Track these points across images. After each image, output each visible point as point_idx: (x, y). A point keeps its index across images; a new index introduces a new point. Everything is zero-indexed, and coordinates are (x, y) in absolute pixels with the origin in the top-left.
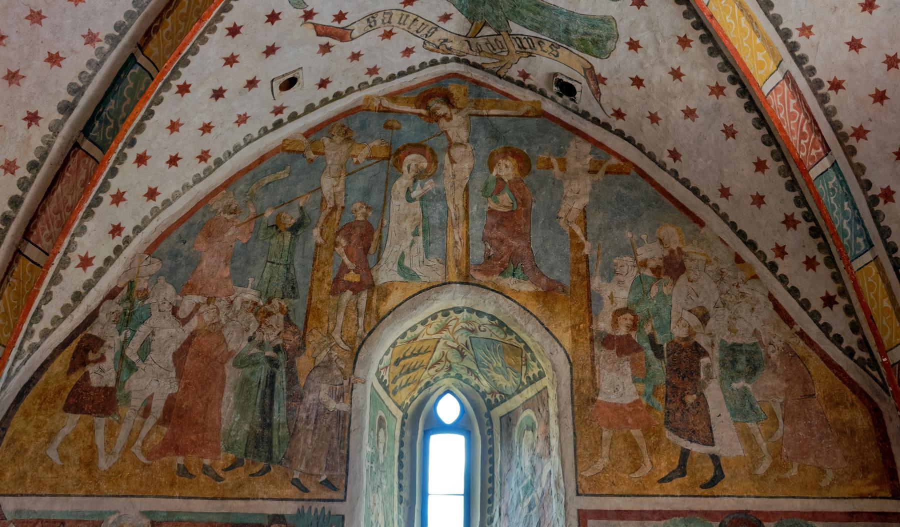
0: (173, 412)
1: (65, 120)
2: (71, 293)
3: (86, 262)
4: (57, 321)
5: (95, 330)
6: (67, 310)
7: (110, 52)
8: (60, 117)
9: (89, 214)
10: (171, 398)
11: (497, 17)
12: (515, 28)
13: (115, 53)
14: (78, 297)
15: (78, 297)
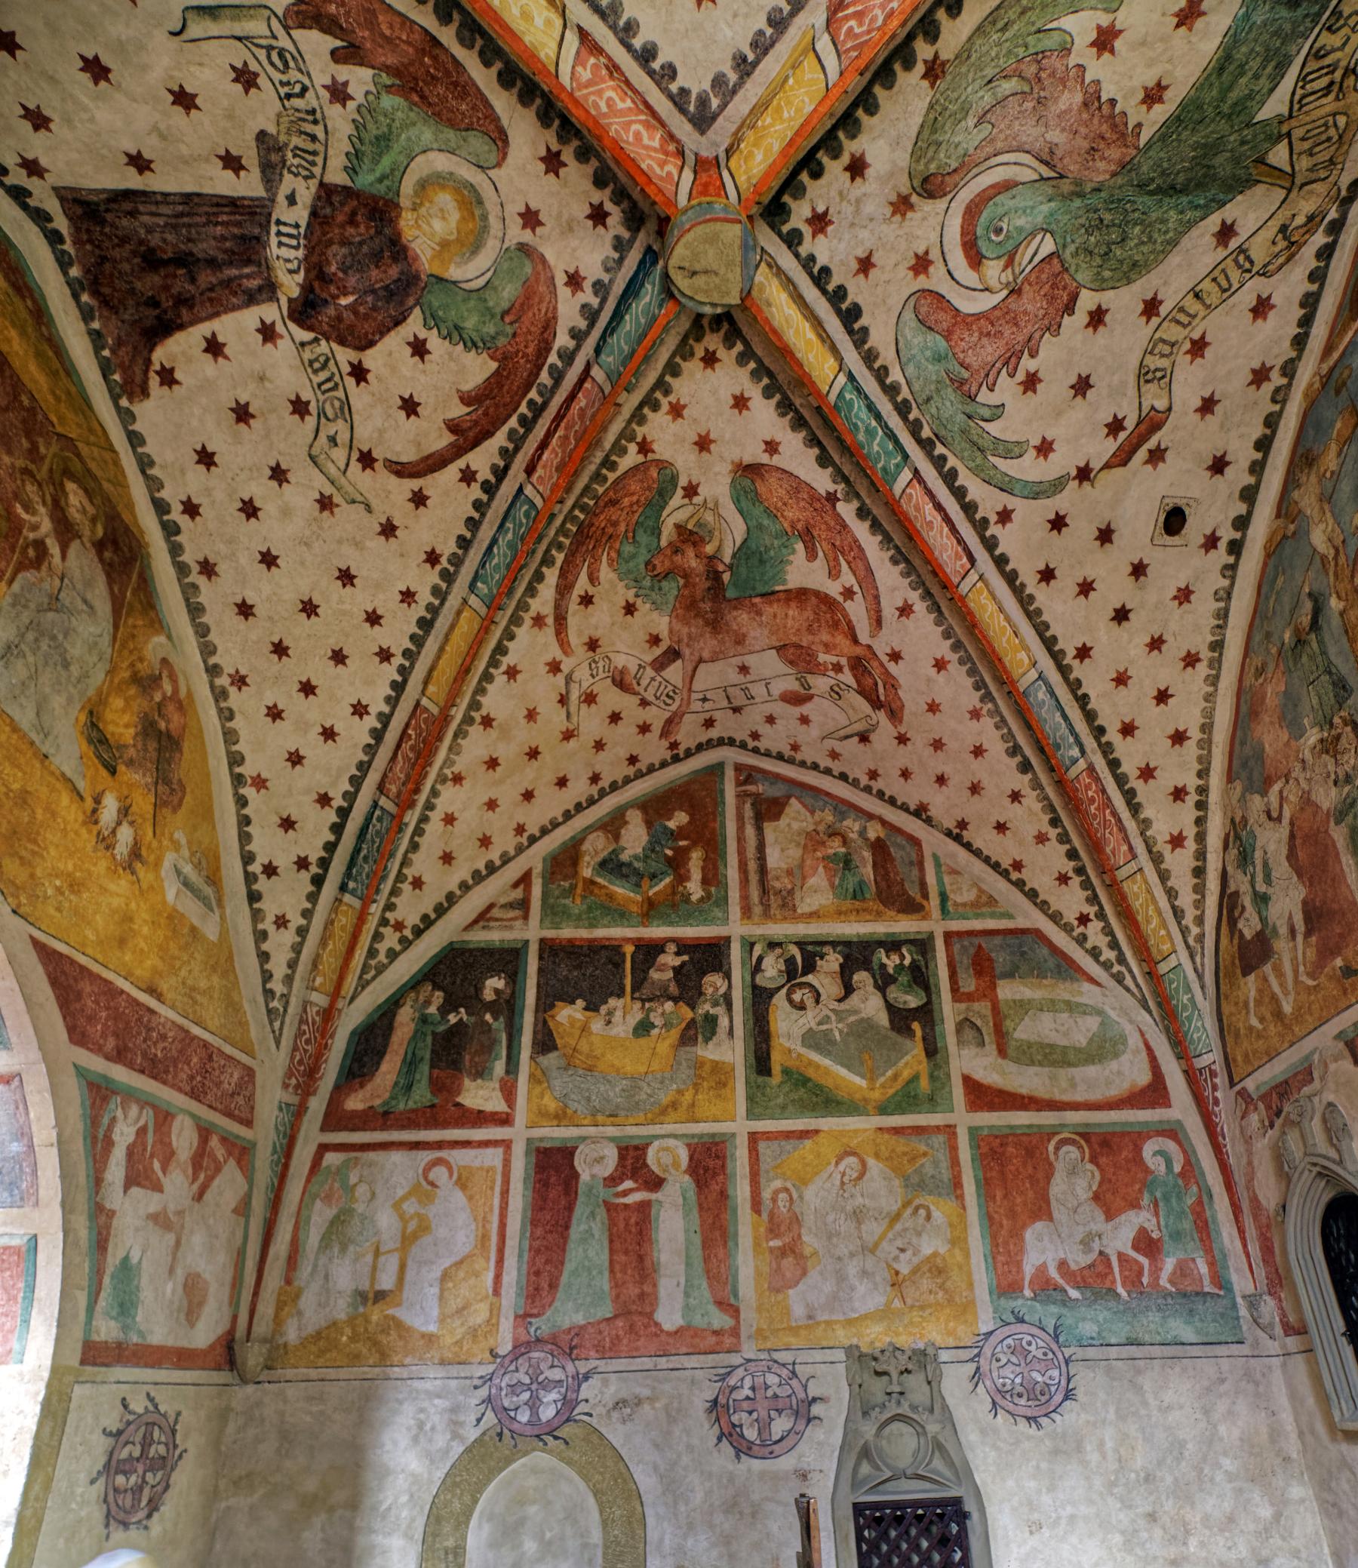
0: (1315, 916)
1: (1034, 773)
2: (1189, 874)
3: (1177, 841)
4: (1199, 904)
5: (1232, 888)
6: (1200, 889)
7: (996, 705)
8: (1030, 775)
9: (1135, 809)
10: (1305, 903)
11: (1243, 143)
12: (1275, 105)
13: (1000, 702)
14: (1199, 872)
15: (1199, 872)
